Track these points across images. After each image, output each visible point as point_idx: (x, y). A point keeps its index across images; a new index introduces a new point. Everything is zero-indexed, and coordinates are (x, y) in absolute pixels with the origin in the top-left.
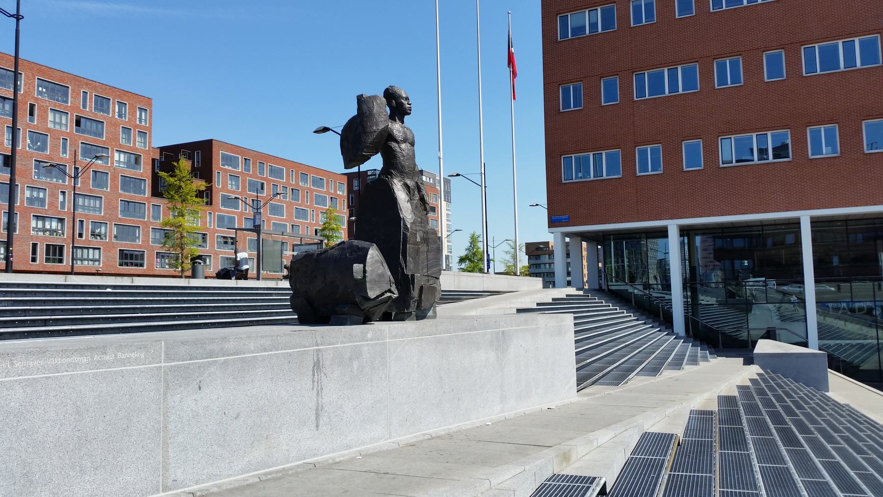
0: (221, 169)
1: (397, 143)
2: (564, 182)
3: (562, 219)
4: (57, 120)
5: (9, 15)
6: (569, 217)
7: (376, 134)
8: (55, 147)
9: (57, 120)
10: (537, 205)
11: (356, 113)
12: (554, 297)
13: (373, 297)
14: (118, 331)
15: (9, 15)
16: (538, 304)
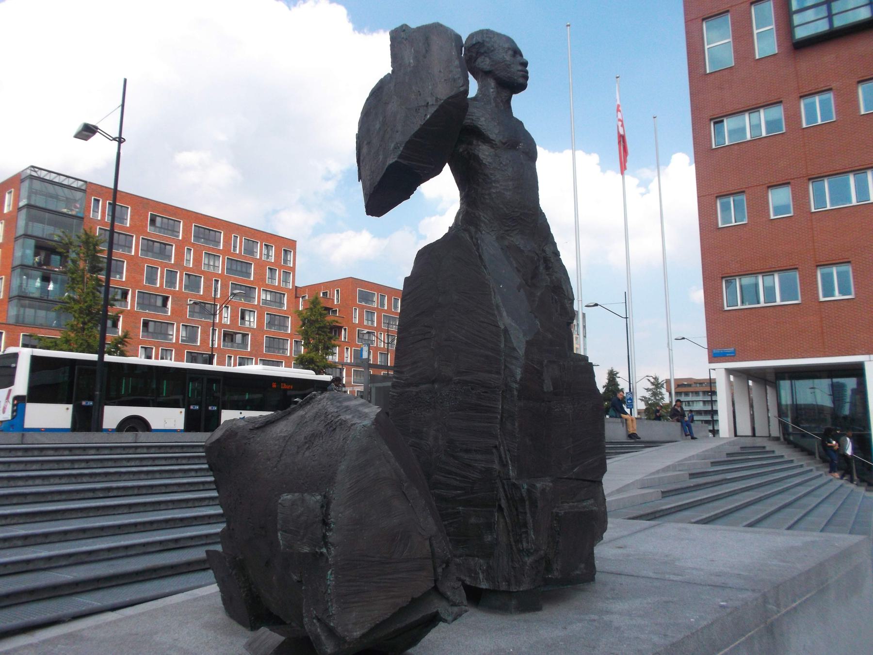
0: (359, 306)
1: (492, 147)
2: (726, 308)
3: (728, 353)
4: (212, 263)
5: (111, 139)
6: (735, 350)
7: (432, 110)
8: (207, 288)
9: (212, 263)
10: (683, 338)
11: (389, 70)
12: (728, 452)
13: (357, 634)
14: (20, 543)
15: (111, 139)
16: (714, 464)
